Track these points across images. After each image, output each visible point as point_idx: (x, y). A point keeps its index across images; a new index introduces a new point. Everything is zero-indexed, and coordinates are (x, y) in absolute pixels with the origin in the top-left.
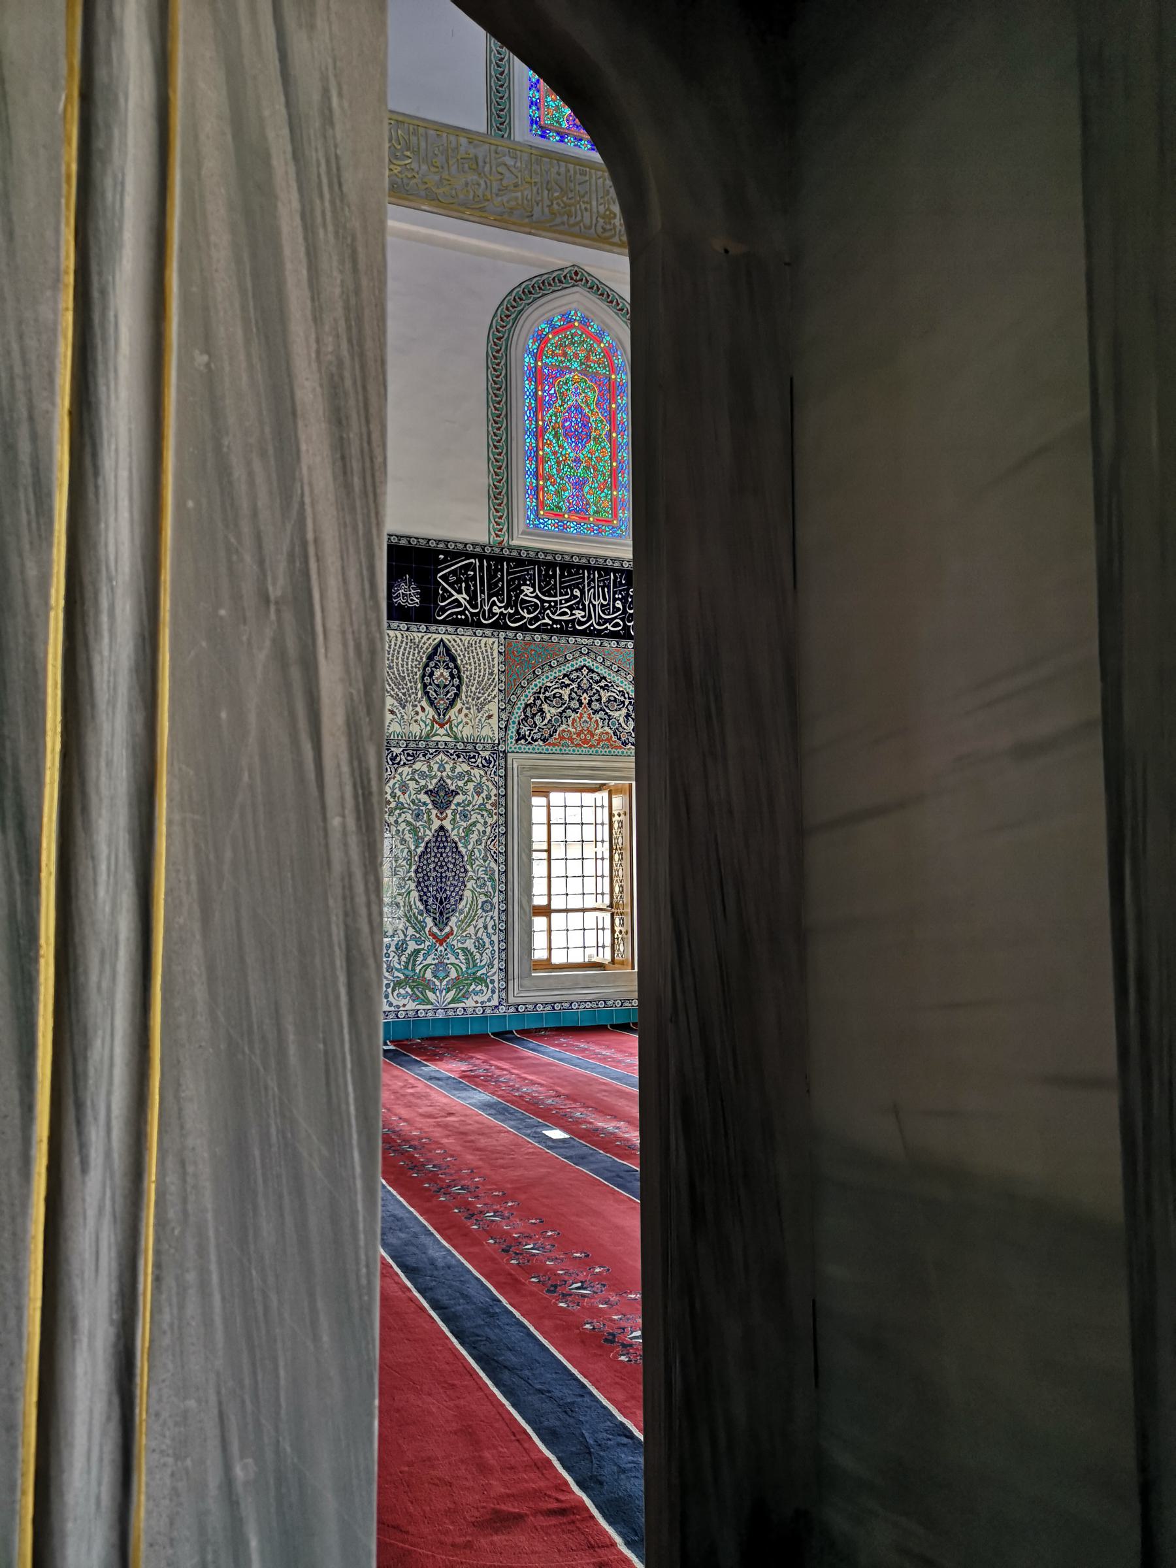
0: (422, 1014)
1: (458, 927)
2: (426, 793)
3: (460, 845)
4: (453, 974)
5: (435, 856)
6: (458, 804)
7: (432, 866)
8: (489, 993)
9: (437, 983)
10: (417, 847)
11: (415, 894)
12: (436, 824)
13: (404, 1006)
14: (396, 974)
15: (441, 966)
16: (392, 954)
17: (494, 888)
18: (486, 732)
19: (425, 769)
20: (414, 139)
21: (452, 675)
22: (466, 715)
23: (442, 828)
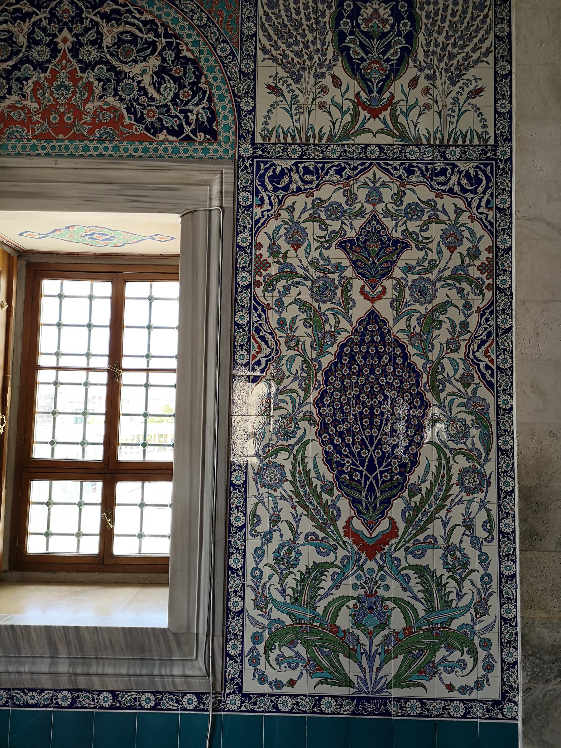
1: (408, 522)
2: (340, 246)
3: (411, 350)
4: (398, 622)
5: (360, 373)
6: (409, 268)
7: (353, 393)
8: (480, 671)
9: (364, 639)
10: (322, 353)
11: (315, 450)
12: (361, 308)
13: (291, 683)
14: (276, 614)
16: (267, 571)
17: (486, 441)
18: (468, 122)
19: (339, 198)
21: (397, 15)
22: (426, 91)
23: (373, 315)
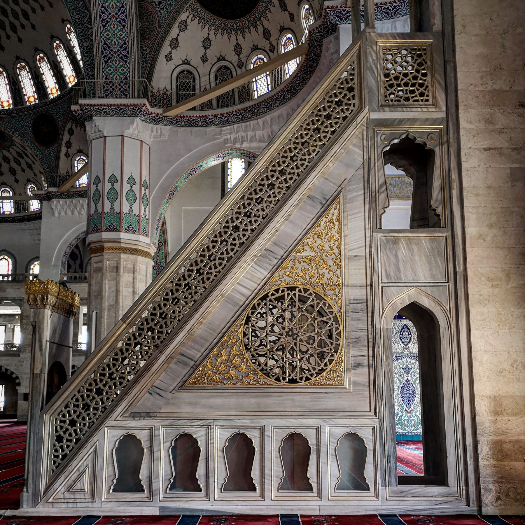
0: (404, 434)
4: (413, 422)
11: (400, 399)
12: (406, 378)
15: (409, 420)
20: (392, 182)
21: (409, 334)
23: (407, 379)
